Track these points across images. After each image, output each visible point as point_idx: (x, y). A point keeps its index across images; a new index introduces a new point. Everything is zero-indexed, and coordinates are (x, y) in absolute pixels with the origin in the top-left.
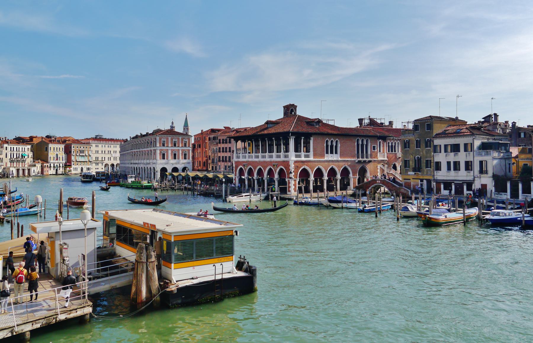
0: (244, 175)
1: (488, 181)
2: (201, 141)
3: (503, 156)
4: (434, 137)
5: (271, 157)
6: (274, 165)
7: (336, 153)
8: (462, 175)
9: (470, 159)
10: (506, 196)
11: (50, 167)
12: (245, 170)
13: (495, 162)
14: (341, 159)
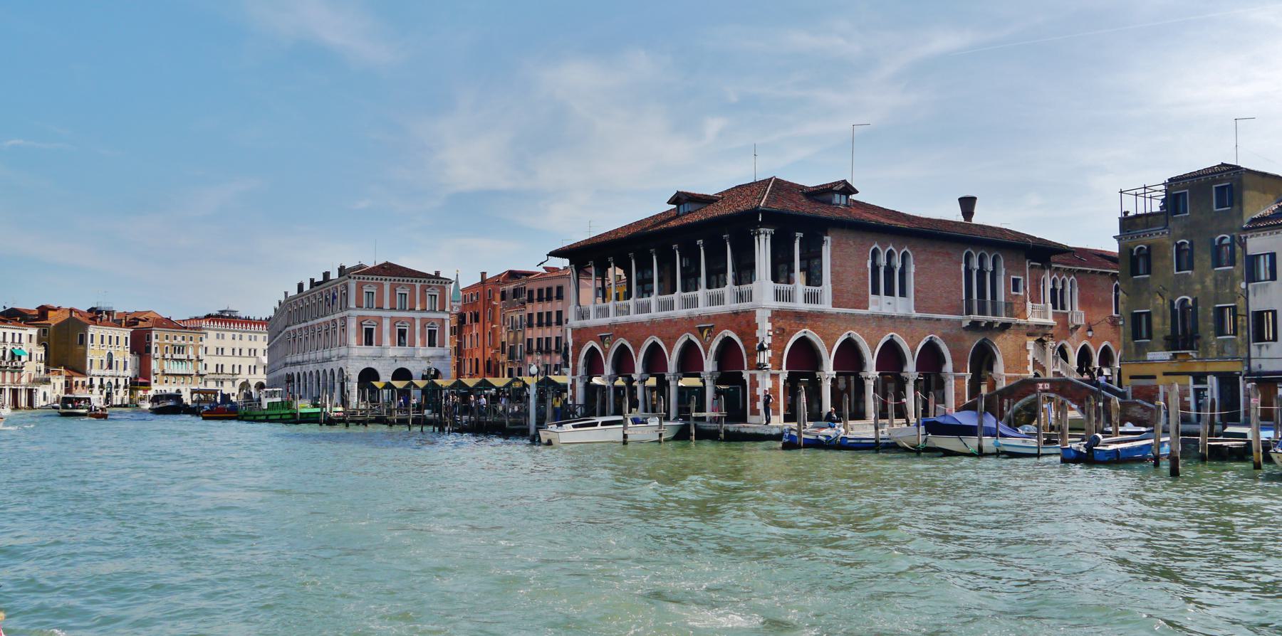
0: (600, 372)
2: (480, 304)
5: (693, 303)
6: (701, 330)
7: (903, 293)
11: (91, 386)
12: (606, 355)
14: (919, 315)
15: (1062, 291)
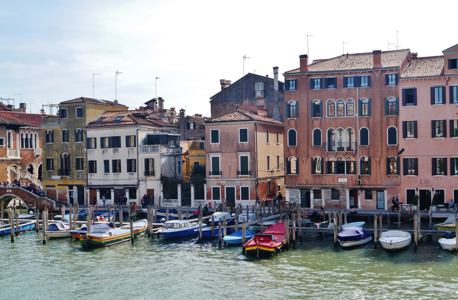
1: (155, 185)
3: (173, 153)
4: (87, 127)
8: (124, 178)
9: (133, 156)
10: (177, 203)
13: (164, 160)
15: (31, 139)
